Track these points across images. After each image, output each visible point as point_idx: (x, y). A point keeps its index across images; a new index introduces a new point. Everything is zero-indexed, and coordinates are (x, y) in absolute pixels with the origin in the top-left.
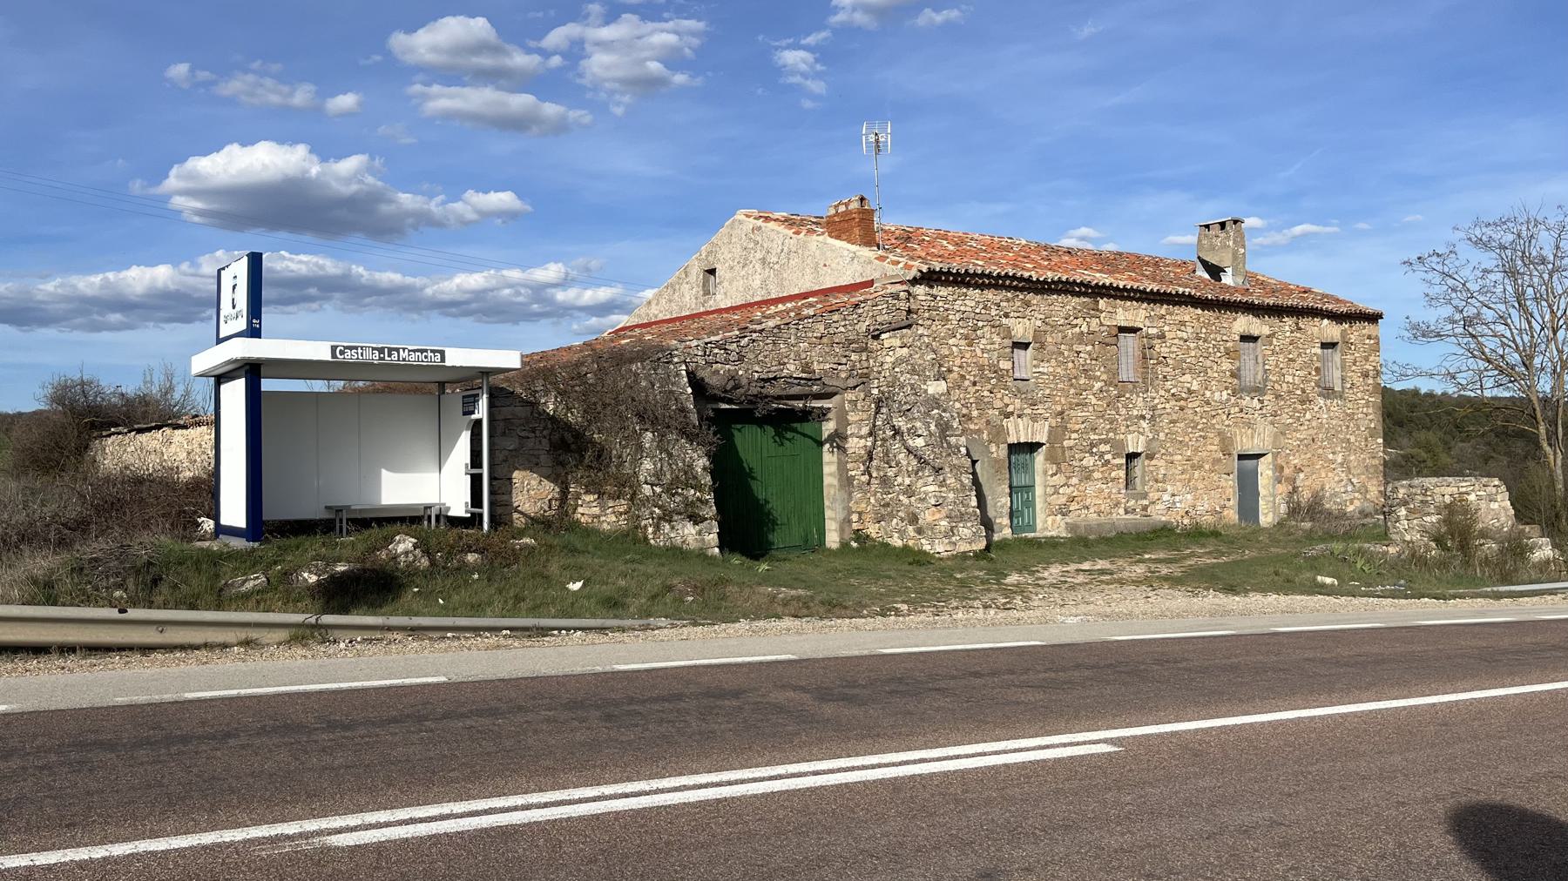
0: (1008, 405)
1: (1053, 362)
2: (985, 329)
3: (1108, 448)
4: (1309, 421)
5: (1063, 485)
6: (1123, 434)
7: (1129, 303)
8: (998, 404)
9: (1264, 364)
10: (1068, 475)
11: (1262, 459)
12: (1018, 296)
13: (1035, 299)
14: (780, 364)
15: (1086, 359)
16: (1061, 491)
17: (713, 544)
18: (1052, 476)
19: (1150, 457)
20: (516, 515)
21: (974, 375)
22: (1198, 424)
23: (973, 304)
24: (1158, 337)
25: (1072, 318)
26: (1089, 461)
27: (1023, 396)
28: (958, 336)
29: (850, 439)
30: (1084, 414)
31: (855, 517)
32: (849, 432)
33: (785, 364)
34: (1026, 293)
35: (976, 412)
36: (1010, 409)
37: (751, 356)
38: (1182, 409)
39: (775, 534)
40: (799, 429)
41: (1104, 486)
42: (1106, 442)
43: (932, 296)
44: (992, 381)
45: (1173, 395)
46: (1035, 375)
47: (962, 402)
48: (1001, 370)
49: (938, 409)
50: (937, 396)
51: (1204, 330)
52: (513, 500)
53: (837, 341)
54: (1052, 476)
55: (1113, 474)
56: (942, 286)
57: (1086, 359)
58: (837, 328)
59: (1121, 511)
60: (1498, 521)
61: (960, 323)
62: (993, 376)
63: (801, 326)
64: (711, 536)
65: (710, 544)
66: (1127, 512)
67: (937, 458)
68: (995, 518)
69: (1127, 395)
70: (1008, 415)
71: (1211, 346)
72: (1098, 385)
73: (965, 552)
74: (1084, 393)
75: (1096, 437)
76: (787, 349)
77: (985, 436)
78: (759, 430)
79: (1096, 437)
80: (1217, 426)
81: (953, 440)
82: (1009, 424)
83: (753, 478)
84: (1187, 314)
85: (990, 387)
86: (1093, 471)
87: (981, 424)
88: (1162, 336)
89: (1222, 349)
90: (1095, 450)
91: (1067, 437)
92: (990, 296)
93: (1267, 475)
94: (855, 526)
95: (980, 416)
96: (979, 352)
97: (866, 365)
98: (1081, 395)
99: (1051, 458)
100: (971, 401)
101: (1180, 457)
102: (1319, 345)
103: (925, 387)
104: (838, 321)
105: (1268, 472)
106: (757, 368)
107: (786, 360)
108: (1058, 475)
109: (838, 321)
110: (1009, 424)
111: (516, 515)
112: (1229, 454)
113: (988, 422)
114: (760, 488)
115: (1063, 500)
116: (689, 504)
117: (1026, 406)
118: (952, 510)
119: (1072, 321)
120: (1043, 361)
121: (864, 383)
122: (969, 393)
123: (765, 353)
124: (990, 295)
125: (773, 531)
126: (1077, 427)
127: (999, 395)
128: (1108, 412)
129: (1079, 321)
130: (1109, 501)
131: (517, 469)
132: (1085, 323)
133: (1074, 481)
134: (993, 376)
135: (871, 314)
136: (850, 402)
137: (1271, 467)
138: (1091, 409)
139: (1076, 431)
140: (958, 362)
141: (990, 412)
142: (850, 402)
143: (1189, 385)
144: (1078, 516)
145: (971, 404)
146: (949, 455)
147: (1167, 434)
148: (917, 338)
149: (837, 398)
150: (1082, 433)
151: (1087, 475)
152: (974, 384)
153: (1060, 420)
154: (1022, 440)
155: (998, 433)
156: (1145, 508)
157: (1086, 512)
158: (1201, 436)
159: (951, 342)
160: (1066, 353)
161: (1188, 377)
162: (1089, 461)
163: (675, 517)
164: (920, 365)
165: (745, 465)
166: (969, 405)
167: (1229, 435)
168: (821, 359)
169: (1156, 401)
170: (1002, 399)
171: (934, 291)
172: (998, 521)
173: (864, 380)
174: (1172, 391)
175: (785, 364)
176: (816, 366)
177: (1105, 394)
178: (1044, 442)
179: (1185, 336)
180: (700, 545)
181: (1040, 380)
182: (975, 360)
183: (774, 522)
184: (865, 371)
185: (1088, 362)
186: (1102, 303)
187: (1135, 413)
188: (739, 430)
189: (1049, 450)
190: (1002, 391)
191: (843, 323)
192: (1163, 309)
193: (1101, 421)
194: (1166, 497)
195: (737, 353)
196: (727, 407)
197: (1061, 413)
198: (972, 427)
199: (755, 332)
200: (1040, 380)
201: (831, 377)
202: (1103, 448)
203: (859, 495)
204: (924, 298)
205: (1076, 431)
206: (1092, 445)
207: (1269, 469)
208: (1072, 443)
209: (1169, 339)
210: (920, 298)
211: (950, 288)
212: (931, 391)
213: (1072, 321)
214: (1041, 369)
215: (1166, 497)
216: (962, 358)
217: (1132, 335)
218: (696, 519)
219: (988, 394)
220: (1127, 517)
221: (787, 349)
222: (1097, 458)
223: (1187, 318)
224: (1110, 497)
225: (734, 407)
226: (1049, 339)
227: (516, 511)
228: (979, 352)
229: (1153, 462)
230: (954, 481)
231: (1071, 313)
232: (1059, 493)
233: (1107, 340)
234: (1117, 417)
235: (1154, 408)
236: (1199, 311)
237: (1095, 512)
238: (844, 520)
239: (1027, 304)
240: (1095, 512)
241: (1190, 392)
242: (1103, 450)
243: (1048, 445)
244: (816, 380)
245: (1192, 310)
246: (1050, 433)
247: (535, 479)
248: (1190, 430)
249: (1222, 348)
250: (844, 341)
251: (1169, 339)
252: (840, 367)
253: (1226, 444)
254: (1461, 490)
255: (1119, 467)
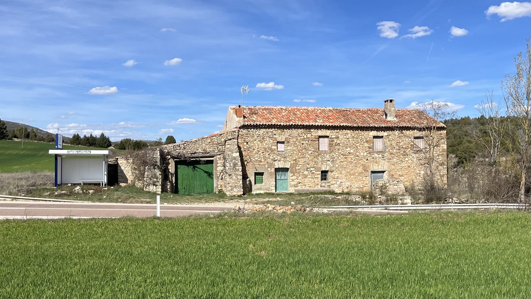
2: (267, 139)
3: (314, 169)
4: (407, 161)
5: (296, 179)
8: (271, 158)
15: (305, 145)
18: (291, 176)
19: (332, 172)
22: (353, 162)
23: (263, 132)
24: (336, 138)
25: (300, 134)
26: (306, 173)
27: (281, 156)
28: (257, 141)
41: (312, 180)
42: (313, 167)
45: (342, 154)
47: (259, 157)
50: (235, 157)
54: (291, 176)
55: (316, 176)
57: (305, 145)
59: (319, 186)
66: (321, 187)
69: (322, 155)
70: (275, 161)
72: (310, 152)
75: (310, 166)
77: (266, 166)
79: (310, 166)
80: (361, 163)
81: (237, 168)
85: (268, 153)
88: (337, 138)
89: (364, 140)
90: (308, 170)
91: (298, 166)
94: (219, 188)
96: (265, 145)
97: (224, 149)
100: (261, 157)
102: (413, 138)
106: (189, 150)
107: (198, 148)
108: (294, 176)
112: (367, 171)
113: (267, 163)
115: (296, 183)
117: (282, 158)
121: (223, 153)
122: (261, 155)
123: (192, 147)
126: (301, 164)
128: (314, 159)
129: (303, 135)
133: (300, 178)
135: (226, 136)
136: (218, 158)
138: (307, 158)
140: (257, 147)
142: (218, 158)
143: (349, 151)
145: (261, 158)
147: (339, 165)
149: (215, 157)
151: (306, 176)
152: (263, 153)
154: (280, 167)
156: (329, 186)
157: (305, 186)
158: (354, 166)
159: (254, 142)
161: (349, 149)
162: (306, 173)
166: (261, 158)
167: (367, 165)
169: (334, 156)
170: (273, 156)
173: (223, 153)
175: (198, 149)
176: (208, 150)
177: (313, 154)
178: (289, 167)
179: (348, 137)
181: (287, 151)
182: (263, 146)
184: (224, 150)
185: (306, 146)
186: (312, 130)
187: (326, 159)
191: (217, 139)
193: (311, 162)
195: (184, 147)
197: (295, 160)
198: (262, 164)
199: (189, 142)
200: (287, 151)
202: (312, 169)
206: (307, 168)
216: (258, 146)
219: (268, 155)
222: (309, 172)
226: (291, 140)
228: (265, 145)
229: (333, 173)
231: (300, 133)
233: (315, 140)
234: (318, 160)
238: (216, 187)
241: (349, 153)
244: (207, 153)
246: (291, 165)
252: (215, 150)
255: (318, 174)
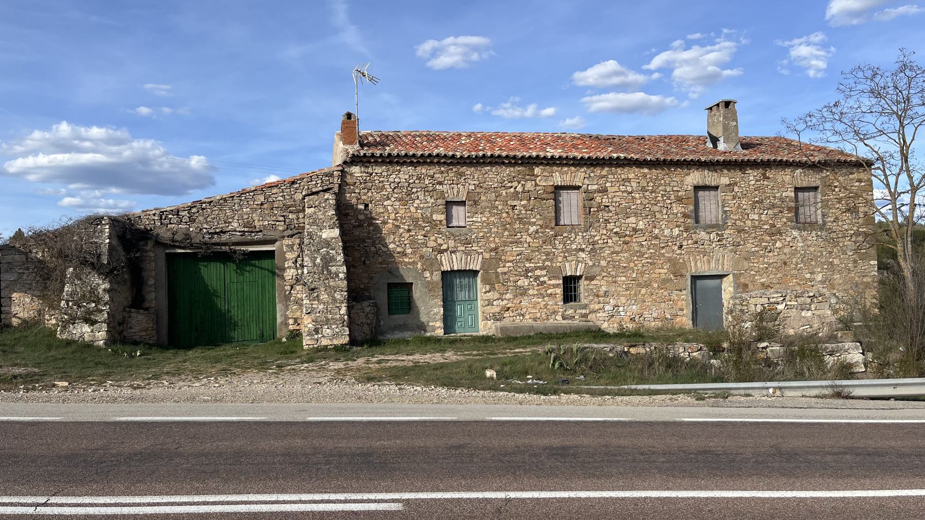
0: (442, 245)
1: (487, 214)
2: (419, 194)
3: (544, 272)
4: (779, 249)
5: (498, 299)
6: (560, 262)
7: (566, 169)
8: (432, 244)
9: (723, 206)
10: (501, 292)
11: (725, 279)
12: (452, 169)
13: (468, 171)
14: (225, 222)
15: (521, 211)
16: (495, 303)
17: (100, 338)
18: (485, 293)
19: (591, 278)
20: (14, 319)
21: (408, 225)
22: (644, 254)
23: (407, 177)
24: (599, 191)
25: (506, 182)
26: (523, 282)
27: (457, 238)
28: (393, 199)
29: (288, 270)
30: (518, 249)
31: (291, 321)
32: (286, 266)
33: (230, 223)
34: (458, 167)
35: (410, 250)
36: (444, 247)
37: (201, 218)
38: (626, 243)
39: (236, 332)
40: (257, 264)
41: (540, 300)
42: (541, 268)
43: (367, 173)
44: (425, 229)
45: (616, 233)
46: (469, 223)
47: (397, 243)
48: (434, 221)
49: (327, 248)
50: (329, 240)
51: (651, 184)
52: (12, 310)
53: (276, 206)
54: (485, 293)
55: (549, 292)
56: (376, 166)
57: (521, 211)
58: (276, 198)
59: (559, 318)
60: (811, 327)
61: (395, 190)
62: (427, 225)
63: (243, 198)
64: (101, 333)
65: (98, 338)
66: (564, 318)
67: (315, 281)
68: (428, 322)
69: (565, 235)
70: (442, 252)
71: (660, 195)
72: (532, 229)
73: (327, 346)
74: (519, 234)
75: (532, 265)
76: (231, 213)
77: (419, 266)
78: (222, 266)
79: (532, 265)
80: (666, 255)
81: (333, 269)
82: (444, 258)
83: (217, 296)
84: (632, 173)
85: (424, 232)
86: (529, 289)
87: (416, 258)
88: (604, 191)
89: (672, 197)
90: (530, 274)
91: (502, 265)
92: (424, 171)
93: (104, 290)
94: (291, 327)
95: (414, 253)
96: (413, 210)
97: (302, 221)
98: (516, 235)
99: (485, 281)
100: (405, 242)
101: (623, 278)
102: (793, 189)
103: (321, 234)
104: (277, 193)
105: (730, 289)
106: (205, 226)
107: (231, 220)
108: (492, 292)
109: (277, 193)
110: (444, 258)
111: (14, 319)
112: (682, 276)
113: (422, 257)
114: (223, 302)
115: (497, 310)
116: (89, 312)
117: (459, 245)
118: (319, 316)
119: (506, 184)
120: (476, 213)
121: (301, 233)
122: (404, 237)
123: (213, 216)
124: (423, 170)
125: (235, 330)
126: (511, 258)
127: (432, 238)
128: (544, 247)
129: (515, 184)
130: (545, 310)
131: (16, 292)
132: (520, 185)
133: (508, 296)
134: (427, 225)
135: (306, 187)
136: (287, 246)
137: (732, 284)
138: (526, 245)
139: (511, 261)
140: (393, 216)
141: (424, 250)
142: (287, 246)
143: (634, 226)
144: (509, 320)
145: (405, 245)
146: (328, 279)
147: (609, 262)
148: (322, 201)
149: (277, 244)
150: (517, 262)
151: (523, 292)
152: (409, 231)
153: (494, 254)
154: (456, 268)
155: (431, 264)
156: (585, 316)
157: (521, 318)
158: (648, 262)
159: (385, 203)
160: (500, 207)
161: (632, 219)
162: (523, 282)
163: (77, 321)
164: (321, 219)
165: (210, 288)
166: (403, 245)
167: (681, 261)
168: (261, 218)
169: (596, 238)
170: (435, 241)
171: (370, 170)
172: (431, 324)
173: (300, 231)
174: (614, 230)
175: (230, 223)
176: (256, 223)
177: (540, 234)
178: (478, 269)
179: (629, 189)
180: (91, 339)
181: (473, 227)
182: (409, 215)
183: (236, 324)
184: (302, 225)
185: (523, 212)
186: (537, 170)
187: (574, 247)
188: (205, 266)
189: (482, 276)
190: (436, 235)
191: (281, 194)
192: (605, 171)
193: (537, 253)
194: (607, 308)
195: (189, 217)
196: (183, 251)
197: (496, 249)
198: (407, 260)
199: (205, 203)
200: (473, 227)
201: (270, 229)
202: (538, 272)
203: (295, 307)
204: (359, 175)
205: (511, 261)
206: (527, 271)
207: (731, 286)
208: (506, 270)
209: (611, 192)
210: (356, 175)
211: (384, 167)
212: (324, 236)
213: (506, 184)
214: (474, 219)
215: (607, 308)
216: (396, 214)
217: (576, 191)
218: (92, 323)
219: (422, 237)
220: (564, 322)
221: (231, 213)
222: (531, 280)
223: (631, 176)
224: (546, 308)
225: (188, 251)
226: (483, 198)
227: (15, 316)
228: (413, 210)
229: (594, 282)
230: (327, 296)
231: (505, 179)
232: (493, 305)
233: (543, 196)
234: (553, 250)
235: (594, 243)
236: (646, 170)
237: (530, 318)
238: (282, 323)
239: (462, 174)
240: (530, 318)
241: (635, 230)
242: (539, 274)
243: (481, 271)
244: (257, 232)
245: (637, 170)
246: (483, 263)
247: (28, 298)
248: (636, 258)
249: (673, 196)
250: (282, 206)
251: (611, 192)
252: (277, 223)
253: (677, 270)
254: (771, 300)
255: (555, 286)
